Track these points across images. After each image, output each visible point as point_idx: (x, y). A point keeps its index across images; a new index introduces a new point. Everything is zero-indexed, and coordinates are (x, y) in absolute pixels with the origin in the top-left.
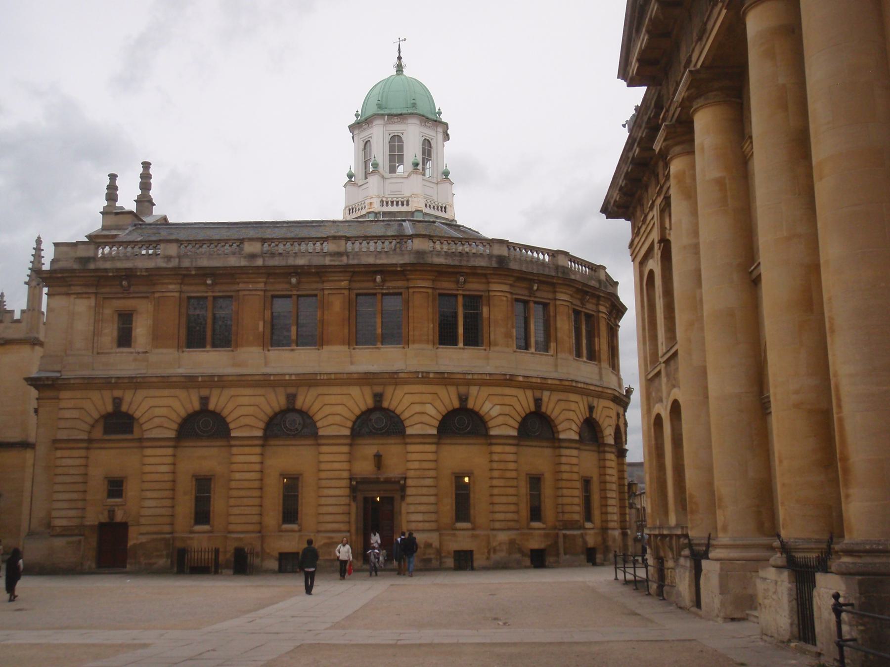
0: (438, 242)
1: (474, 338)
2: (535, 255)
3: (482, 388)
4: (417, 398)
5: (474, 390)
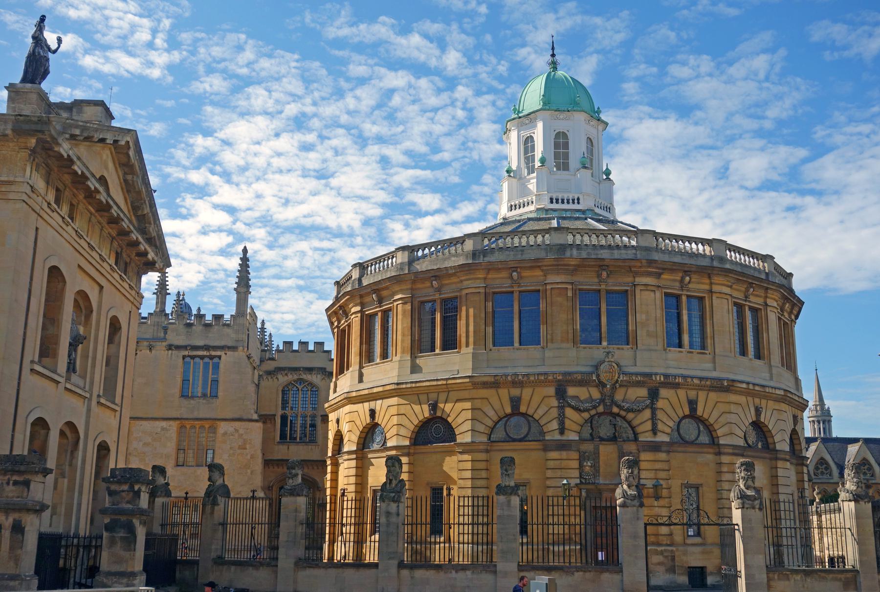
0: (594, 236)
1: (530, 338)
3: (537, 390)
5: (526, 393)
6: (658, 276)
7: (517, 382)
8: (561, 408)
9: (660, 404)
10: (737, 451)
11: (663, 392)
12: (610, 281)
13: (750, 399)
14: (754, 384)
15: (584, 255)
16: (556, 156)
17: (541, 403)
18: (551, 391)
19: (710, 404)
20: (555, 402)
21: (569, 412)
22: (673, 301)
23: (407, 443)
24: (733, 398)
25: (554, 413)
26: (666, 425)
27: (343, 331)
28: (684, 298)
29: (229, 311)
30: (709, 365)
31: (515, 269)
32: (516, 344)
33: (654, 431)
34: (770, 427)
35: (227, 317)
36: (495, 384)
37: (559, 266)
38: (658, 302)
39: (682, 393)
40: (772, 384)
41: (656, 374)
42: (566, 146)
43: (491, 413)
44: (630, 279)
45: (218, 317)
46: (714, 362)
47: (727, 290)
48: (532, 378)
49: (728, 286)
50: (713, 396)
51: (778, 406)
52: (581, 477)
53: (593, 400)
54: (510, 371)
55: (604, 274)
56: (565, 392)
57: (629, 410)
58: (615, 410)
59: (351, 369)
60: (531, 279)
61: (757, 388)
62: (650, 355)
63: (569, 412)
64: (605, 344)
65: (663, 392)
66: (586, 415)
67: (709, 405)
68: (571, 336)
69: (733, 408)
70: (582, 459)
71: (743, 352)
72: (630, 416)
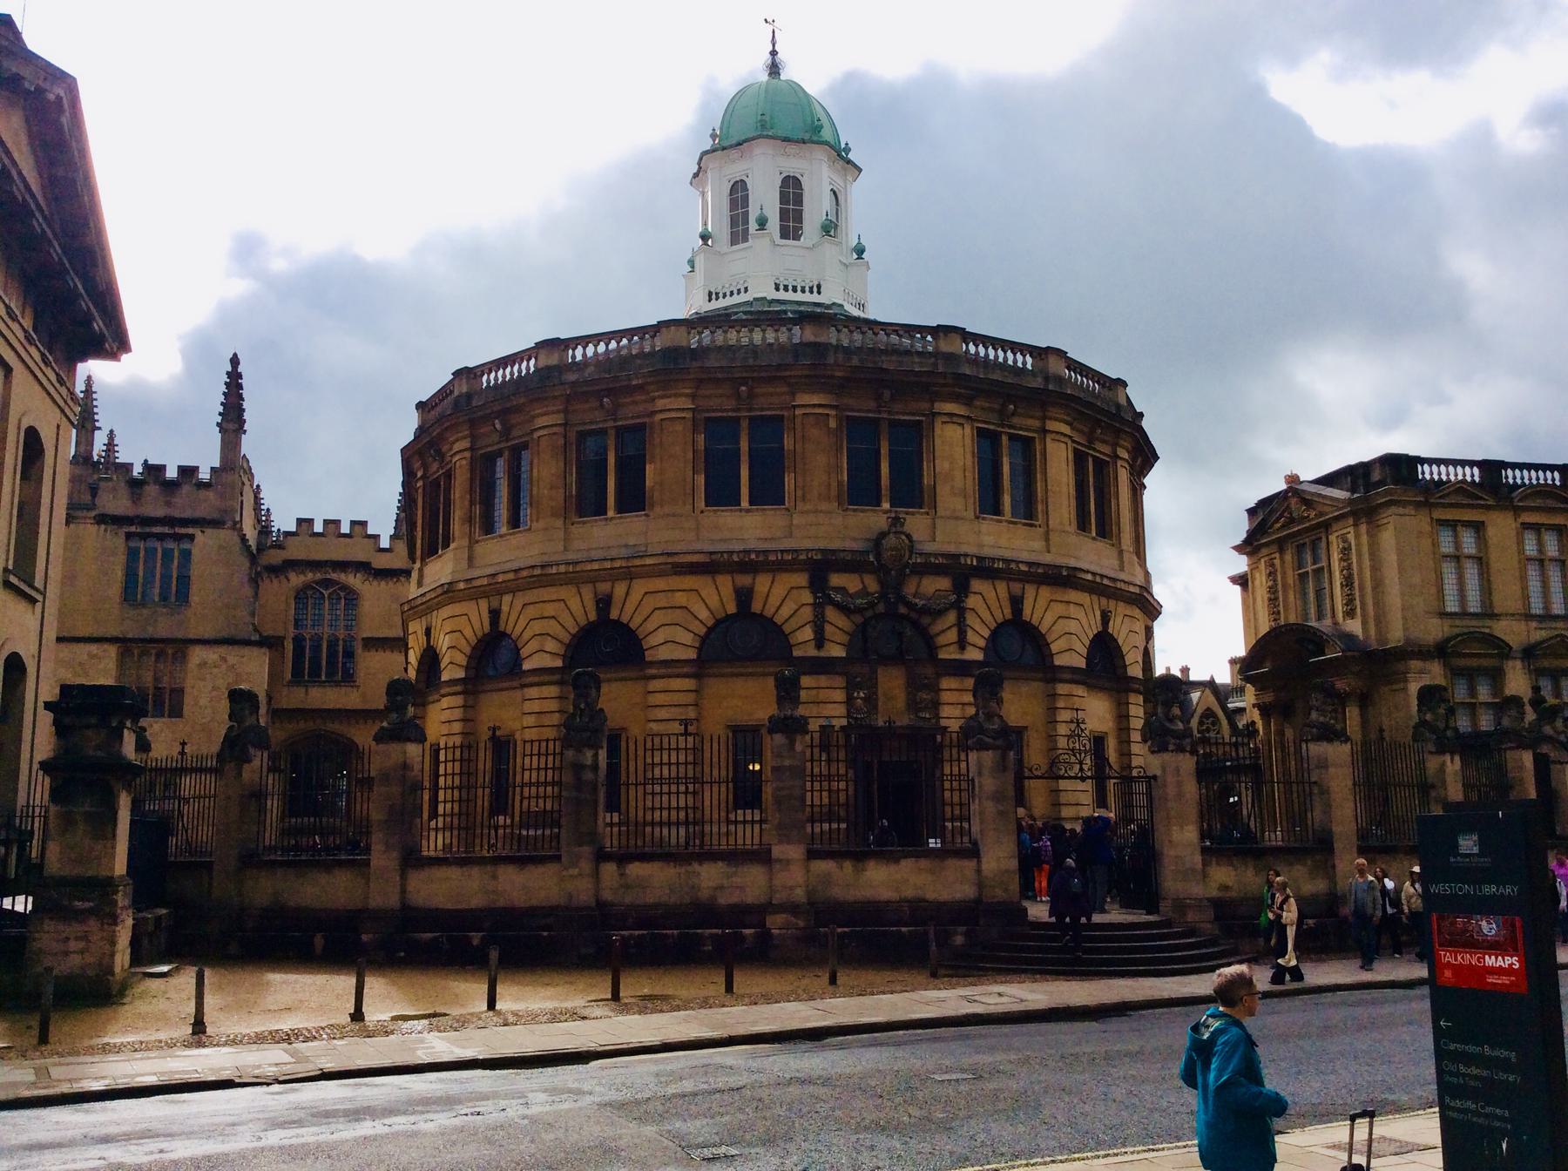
1: (768, 493)
2: (991, 352)
4: (662, 601)
5: (762, 583)
6: (968, 401)
7: (750, 564)
8: (818, 607)
9: (972, 601)
10: (1076, 677)
11: (977, 585)
12: (897, 407)
13: (1095, 598)
14: (1102, 576)
15: (855, 362)
16: (784, 215)
17: (783, 599)
18: (801, 579)
19: (1042, 603)
20: (807, 597)
21: (831, 614)
22: (988, 441)
23: (559, 663)
24: (1074, 595)
25: (807, 613)
26: (979, 634)
27: (436, 483)
28: (1005, 439)
29: (207, 458)
30: (1038, 545)
31: (744, 381)
32: (745, 504)
33: (962, 643)
34: (1120, 642)
35: (204, 475)
36: (709, 567)
37: (816, 382)
38: (968, 441)
39: (1002, 587)
40: (1122, 576)
41: (966, 555)
42: (799, 200)
43: (704, 614)
44: (925, 406)
45: (188, 472)
46: (1047, 540)
47: (1065, 429)
48: (772, 558)
49: (1067, 423)
50: (1045, 593)
52: (849, 716)
53: (868, 594)
54: (738, 547)
55: (887, 394)
56: (825, 580)
57: (925, 611)
58: (903, 610)
59: (452, 546)
60: (769, 401)
61: (1106, 582)
62: (955, 526)
63: (831, 614)
64: (886, 506)
65: (977, 585)
66: (858, 619)
67: (1042, 608)
68: (834, 493)
69: (1073, 611)
70: (850, 687)
71: (1083, 525)
72: (925, 620)
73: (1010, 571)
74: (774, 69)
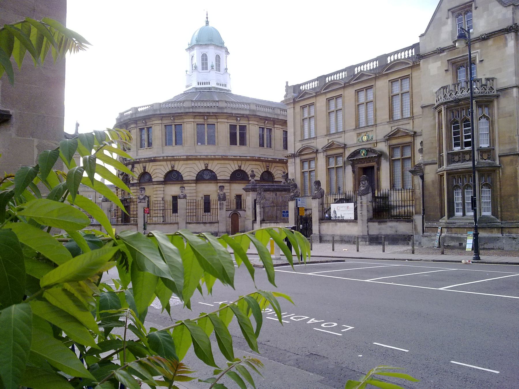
11: (136, 165)
19: (150, 166)
39: (141, 165)
50: (151, 164)
51: (185, 162)
61: (169, 158)
65: (136, 165)
67: (150, 168)
69: (158, 167)
73: (140, 161)
74: (207, 23)
